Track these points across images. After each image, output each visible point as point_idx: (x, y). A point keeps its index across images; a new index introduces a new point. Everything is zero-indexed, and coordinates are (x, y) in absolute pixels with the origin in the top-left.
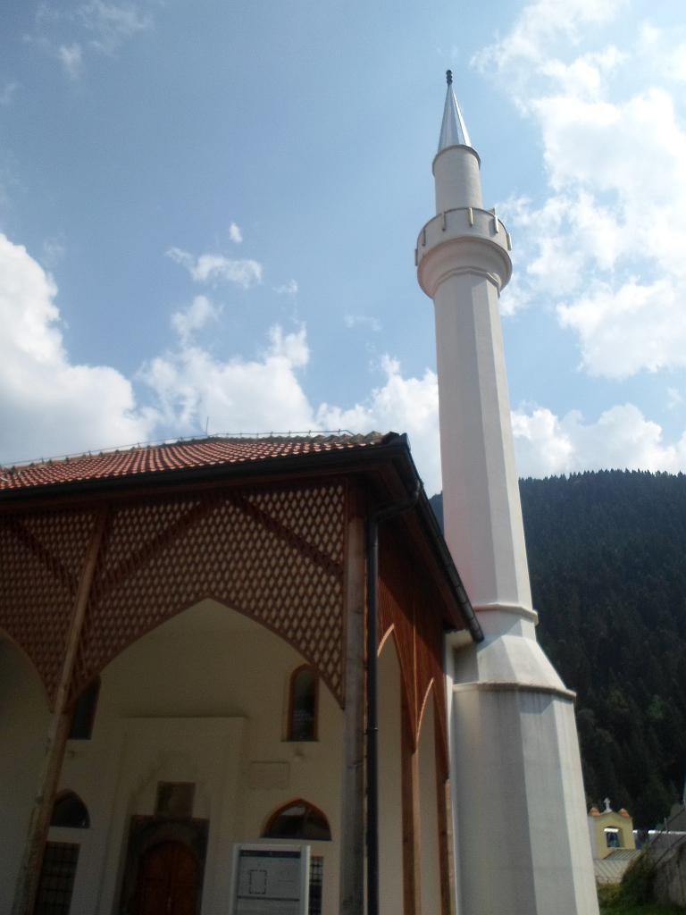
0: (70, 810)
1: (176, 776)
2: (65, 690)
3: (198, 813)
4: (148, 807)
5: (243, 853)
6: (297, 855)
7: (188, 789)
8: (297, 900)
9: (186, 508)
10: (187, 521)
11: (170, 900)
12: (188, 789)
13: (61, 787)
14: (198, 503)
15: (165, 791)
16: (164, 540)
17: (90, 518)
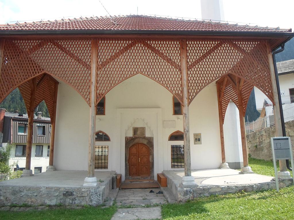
0: (102, 137)
1: (139, 125)
2: (187, 99)
3: (148, 135)
4: (131, 134)
5: (274, 139)
6: (288, 139)
7: (143, 129)
8: (289, 149)
9: (215, 43)
10: (216, 48)
11: (139, 159)
12: (143, 129)
13: (97, 130)
14: (219, 42)
15: (135, 130)
16: (209, 53)
17: (178, 43)
